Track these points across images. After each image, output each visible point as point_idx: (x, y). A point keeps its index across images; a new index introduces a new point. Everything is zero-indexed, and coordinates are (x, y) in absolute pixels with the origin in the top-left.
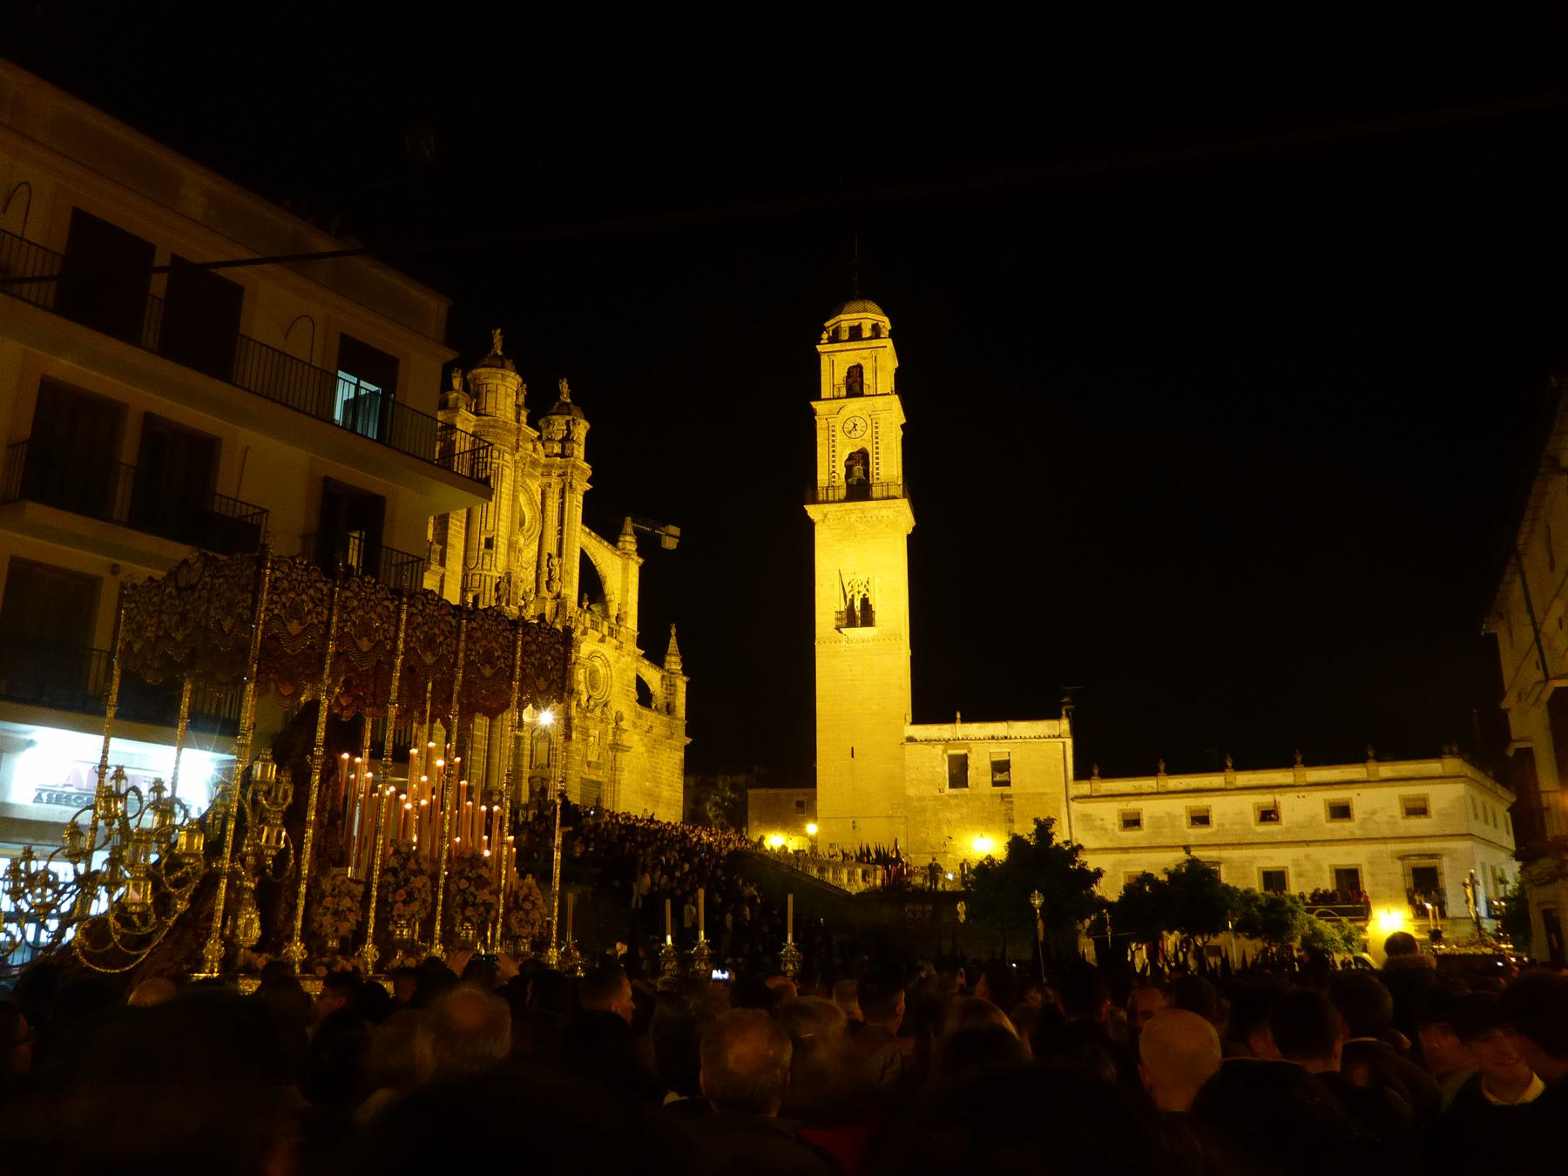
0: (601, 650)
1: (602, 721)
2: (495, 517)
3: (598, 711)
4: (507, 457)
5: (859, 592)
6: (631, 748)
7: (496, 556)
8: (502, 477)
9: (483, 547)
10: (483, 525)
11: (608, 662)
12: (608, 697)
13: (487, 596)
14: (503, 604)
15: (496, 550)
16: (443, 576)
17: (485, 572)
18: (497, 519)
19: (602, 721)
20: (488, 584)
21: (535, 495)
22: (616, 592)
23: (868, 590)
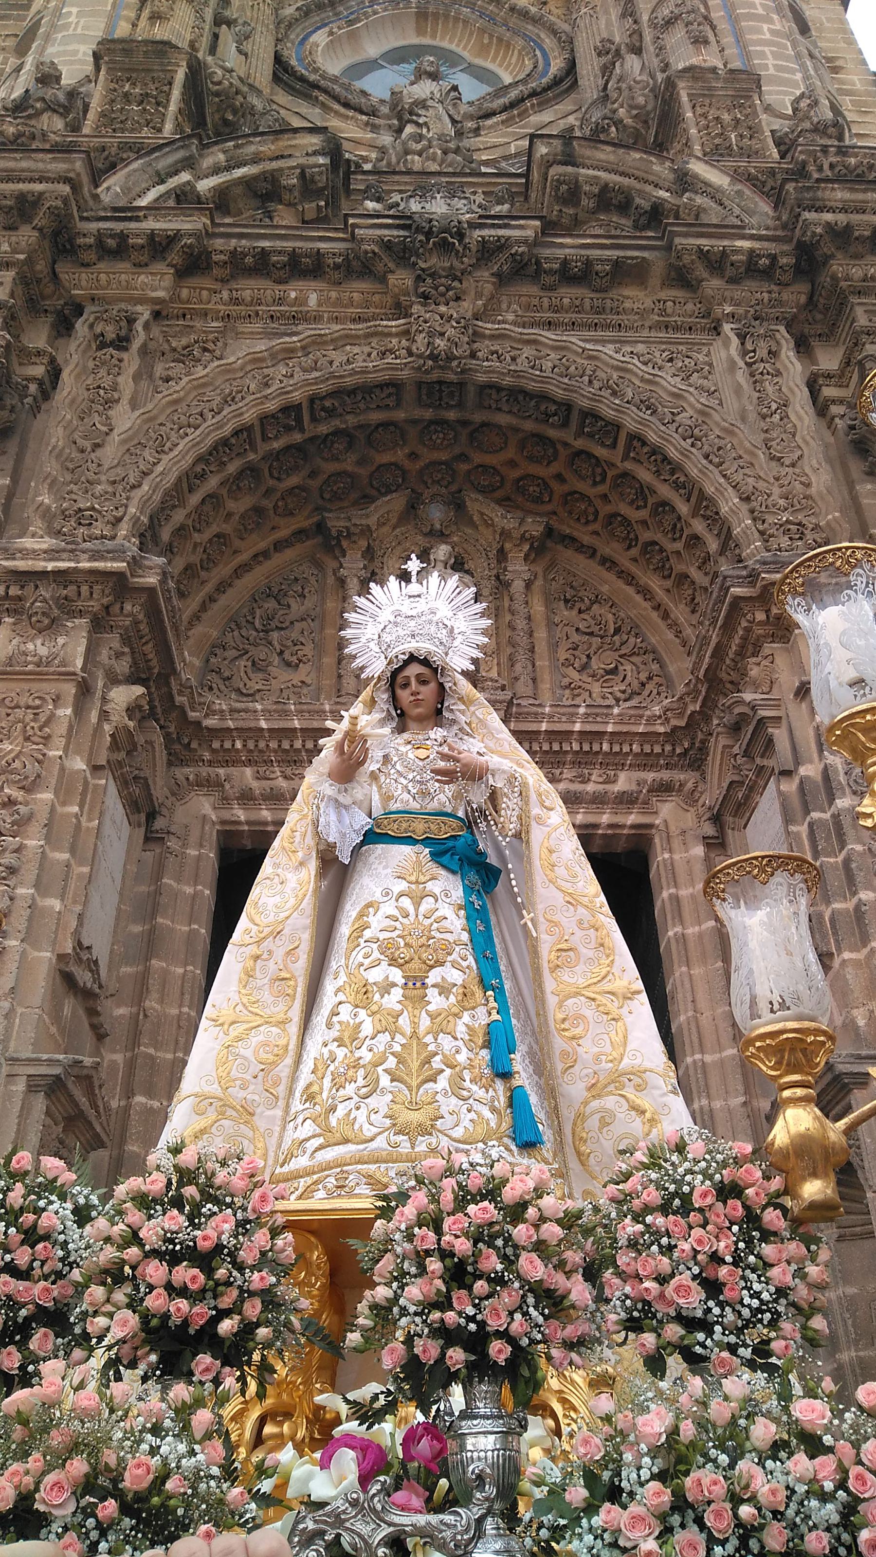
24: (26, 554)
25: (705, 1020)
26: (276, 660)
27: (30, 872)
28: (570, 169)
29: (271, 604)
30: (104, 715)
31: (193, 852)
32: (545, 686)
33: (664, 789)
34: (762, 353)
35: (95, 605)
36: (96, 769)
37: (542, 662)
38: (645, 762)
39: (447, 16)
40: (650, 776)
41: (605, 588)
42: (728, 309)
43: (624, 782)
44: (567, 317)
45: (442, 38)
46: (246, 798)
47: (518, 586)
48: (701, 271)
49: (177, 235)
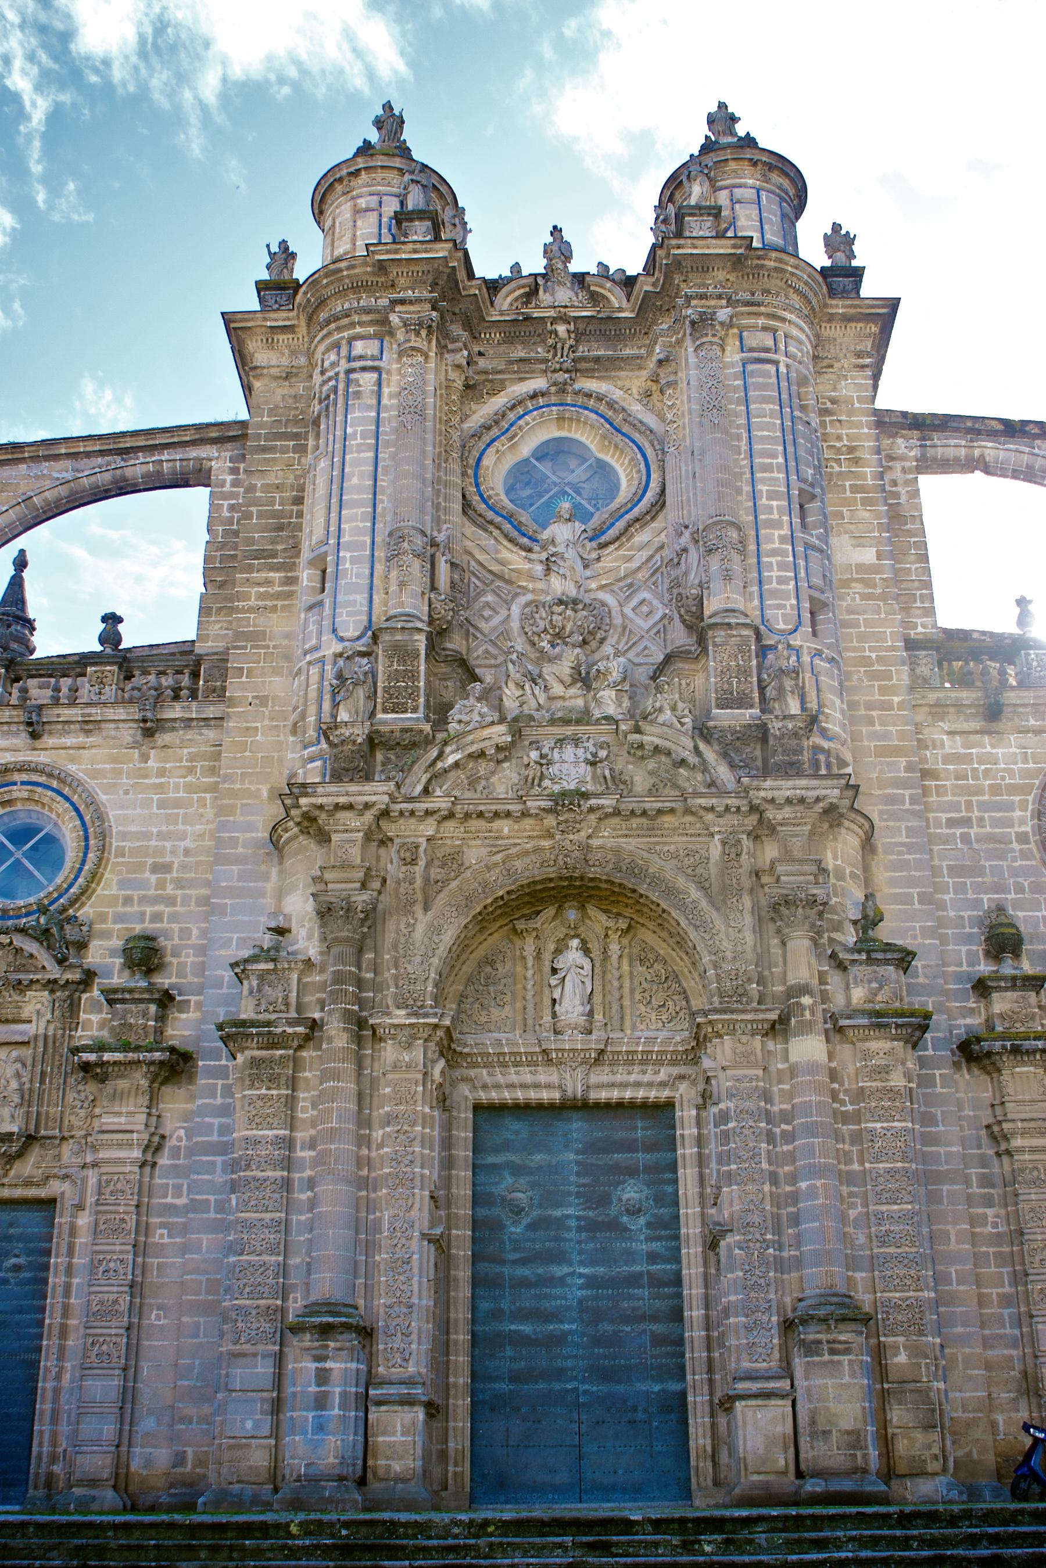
18: (335, 507)
24: (397, 1017)
25: (689, 1194)
26: (493, 1003)
27: (418, 1163)
28: (637, 736)
29: (488, 969)
30: (433, 1081)
31: (463, 1115)
32: (627, 1018)
33: (682, 1077)
34: (733, 856)
35: (426, 1036)
36: (431, 1107)
37: (627, 1002)
38: (674, 1063)
39: (578, 421)
40: (676, 1071)
41: (662, 952)
42: (717, 829)
43: (663, 1074)
44: (635, 833)
45: (576, 432)
46: (485, 1087)
47: (614, 958)
48: (702, 813)
49: (439, 810)
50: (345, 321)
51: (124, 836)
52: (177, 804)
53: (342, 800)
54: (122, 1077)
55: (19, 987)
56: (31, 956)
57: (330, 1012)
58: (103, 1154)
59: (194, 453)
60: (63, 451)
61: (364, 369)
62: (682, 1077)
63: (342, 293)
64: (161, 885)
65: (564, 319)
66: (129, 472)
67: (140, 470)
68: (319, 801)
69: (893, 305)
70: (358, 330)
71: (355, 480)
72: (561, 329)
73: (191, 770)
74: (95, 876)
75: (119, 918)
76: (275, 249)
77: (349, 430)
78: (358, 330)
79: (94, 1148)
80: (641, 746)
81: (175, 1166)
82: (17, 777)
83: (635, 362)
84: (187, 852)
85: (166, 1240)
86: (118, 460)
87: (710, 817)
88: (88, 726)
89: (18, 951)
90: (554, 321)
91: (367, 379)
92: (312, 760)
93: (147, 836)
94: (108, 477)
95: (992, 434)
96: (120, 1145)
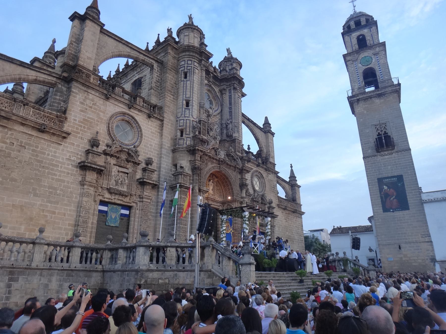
0: (259, 170)
1: (262, 203)
2: (190, 92)
3: (260, 199)
4: (196, 64)
5: (382, 131)
6: (278, 216)
7: (192, 111)
8: (194, 73)
9: (185, 106)
10: (184, 96)
11: (262, 176)
12: (264, 192)
13: (188, 130)
14: (197, 133)
15: (192, 108)
16: (162, 121)
17: (186, 118)
19: (262, 203)
20: (188, 124)
21: (218, 94)
22: (264, 146)
23: (386, 129)
38: (220, 203)
40: (220, 204)
50: (194, 57)
51: (145, 136)
52: (153, 133)
53: (202, 149)
54: (148, 185)
55: (128, 161)
56: (132, 156)
57: (196, 185)
58: (144, 200)
59: (151, 60)
60: (130, 46)
61: (196, 68)
62: (221, 205)
63: (193, 52)
64: (151, 148)
65: (212, 73)
66: (140, 57)
67: (141, 58)
68: (199, 148)
69: (246, 95)
70: (195, 60)
71: (195, 89)
72: (212, 75)
73: (156, 128)
74: (140, 142)
75: (144, 153)
76: (169, 29)
77: (194, 79)
78: (195, 60)
79: (142, 198)
80: (231, 154)
81: (153, 204)
82: (126, 115)
83: (219, 86)
84: (155, 144)
85: (151, 218)
86: (138, 54)
87: (236, 169)
88: (140, 111)
89: (129, 154)
90: (211, 73)
91: (197, 71)
92: (188, 138)
93: (149, 138)
94: (136, 56)
95: (246, 119)
96: (148, 199)
